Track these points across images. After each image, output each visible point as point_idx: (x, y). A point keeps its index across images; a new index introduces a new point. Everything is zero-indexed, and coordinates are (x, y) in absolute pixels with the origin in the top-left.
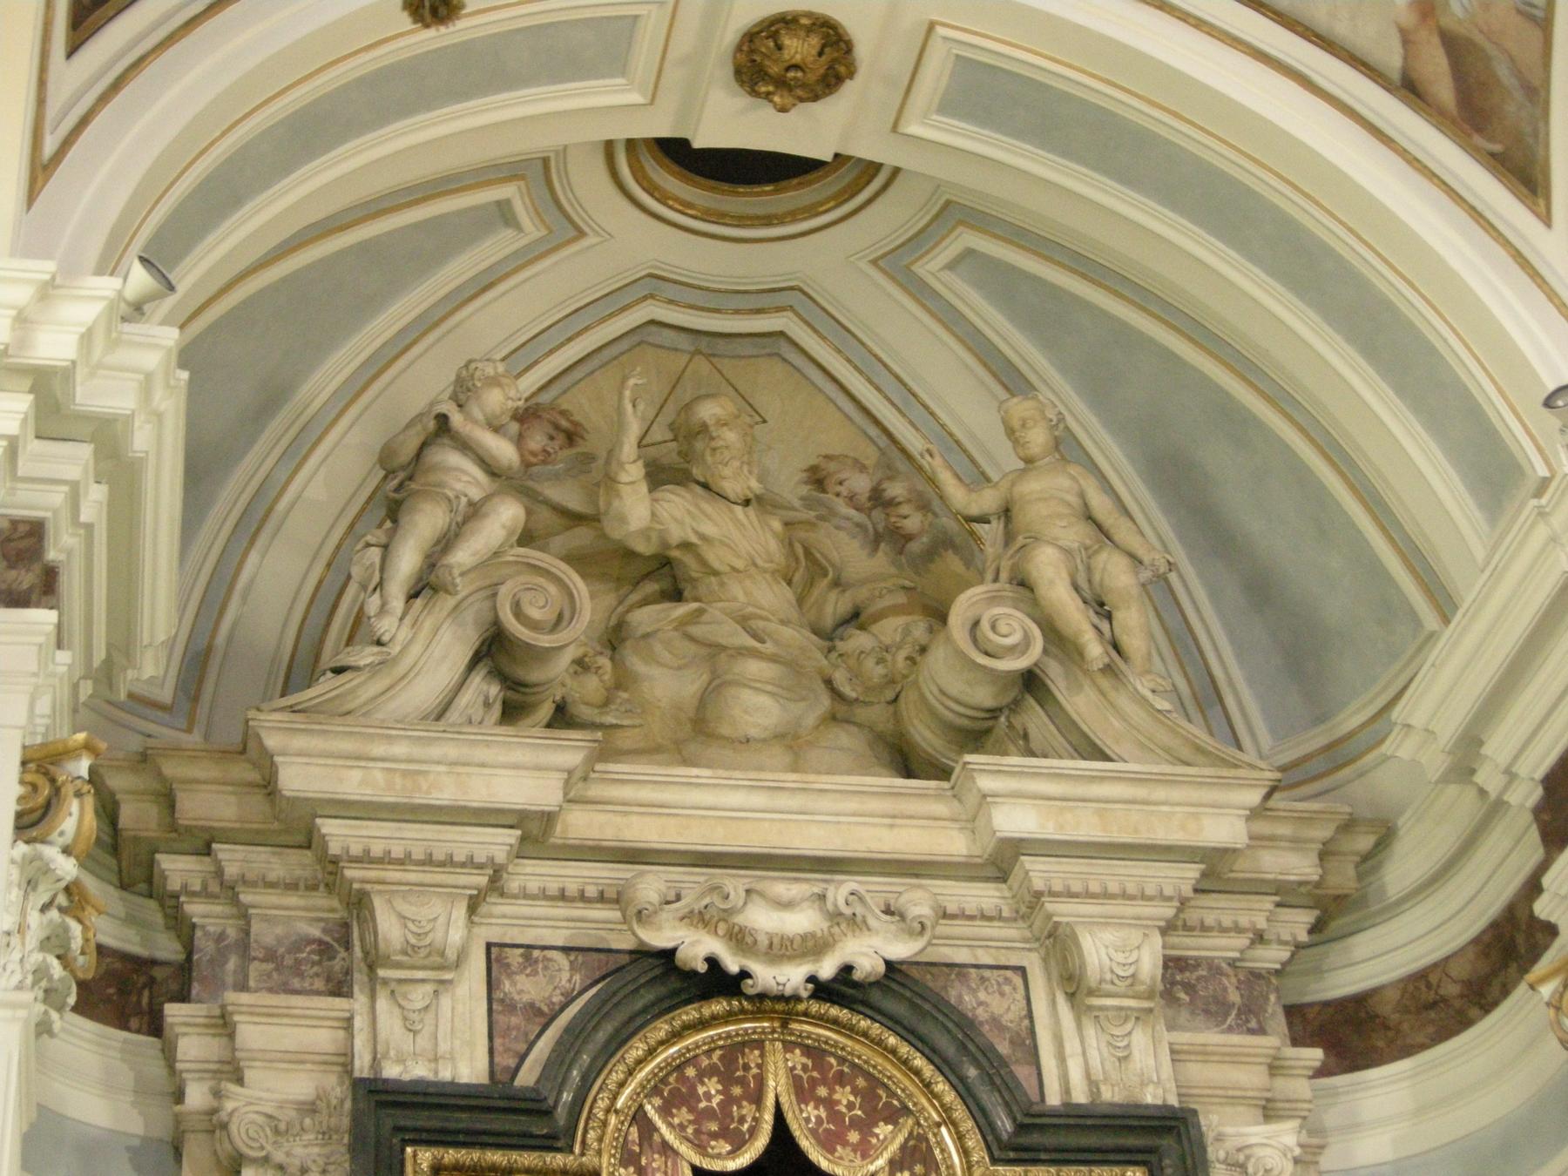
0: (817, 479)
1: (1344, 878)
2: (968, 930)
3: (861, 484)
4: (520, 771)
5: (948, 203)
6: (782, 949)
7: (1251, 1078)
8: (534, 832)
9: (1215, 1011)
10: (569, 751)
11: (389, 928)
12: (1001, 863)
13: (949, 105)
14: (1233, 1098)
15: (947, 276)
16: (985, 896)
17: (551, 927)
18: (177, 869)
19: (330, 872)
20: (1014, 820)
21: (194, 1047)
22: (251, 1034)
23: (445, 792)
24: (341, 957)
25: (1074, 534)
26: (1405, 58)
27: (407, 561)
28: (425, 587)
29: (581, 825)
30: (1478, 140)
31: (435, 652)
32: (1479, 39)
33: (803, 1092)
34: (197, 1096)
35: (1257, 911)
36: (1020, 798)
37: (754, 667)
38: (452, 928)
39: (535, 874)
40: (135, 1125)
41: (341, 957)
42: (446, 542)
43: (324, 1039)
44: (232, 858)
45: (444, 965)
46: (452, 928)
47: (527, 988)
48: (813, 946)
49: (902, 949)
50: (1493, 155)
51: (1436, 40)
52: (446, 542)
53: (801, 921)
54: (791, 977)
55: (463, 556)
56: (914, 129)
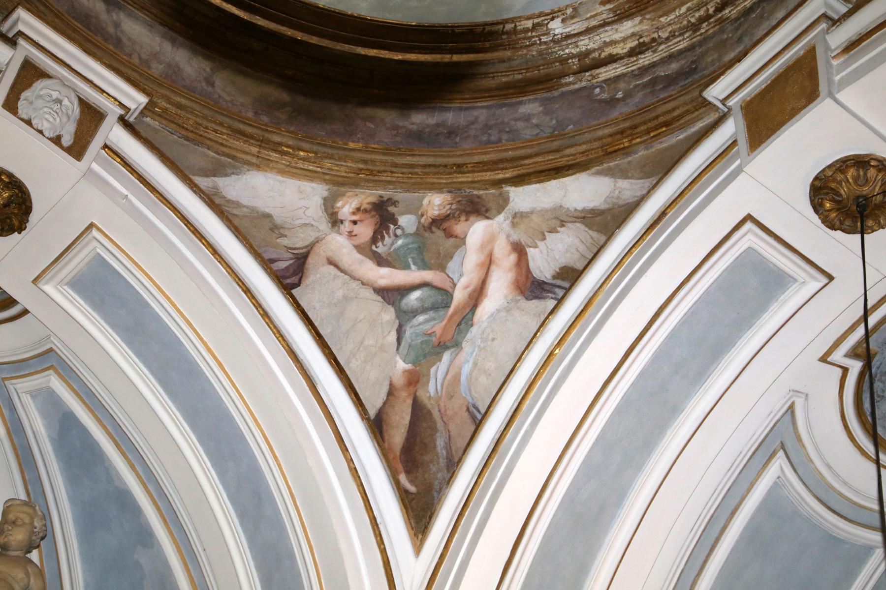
5: (51, 350)
13: (79, 284)
15: (27, 399)
26: (385, 404)
30: (403, 478)
32: (436, 414)
50: (407, 492)
51: (409, 402)
56: (49, 288)
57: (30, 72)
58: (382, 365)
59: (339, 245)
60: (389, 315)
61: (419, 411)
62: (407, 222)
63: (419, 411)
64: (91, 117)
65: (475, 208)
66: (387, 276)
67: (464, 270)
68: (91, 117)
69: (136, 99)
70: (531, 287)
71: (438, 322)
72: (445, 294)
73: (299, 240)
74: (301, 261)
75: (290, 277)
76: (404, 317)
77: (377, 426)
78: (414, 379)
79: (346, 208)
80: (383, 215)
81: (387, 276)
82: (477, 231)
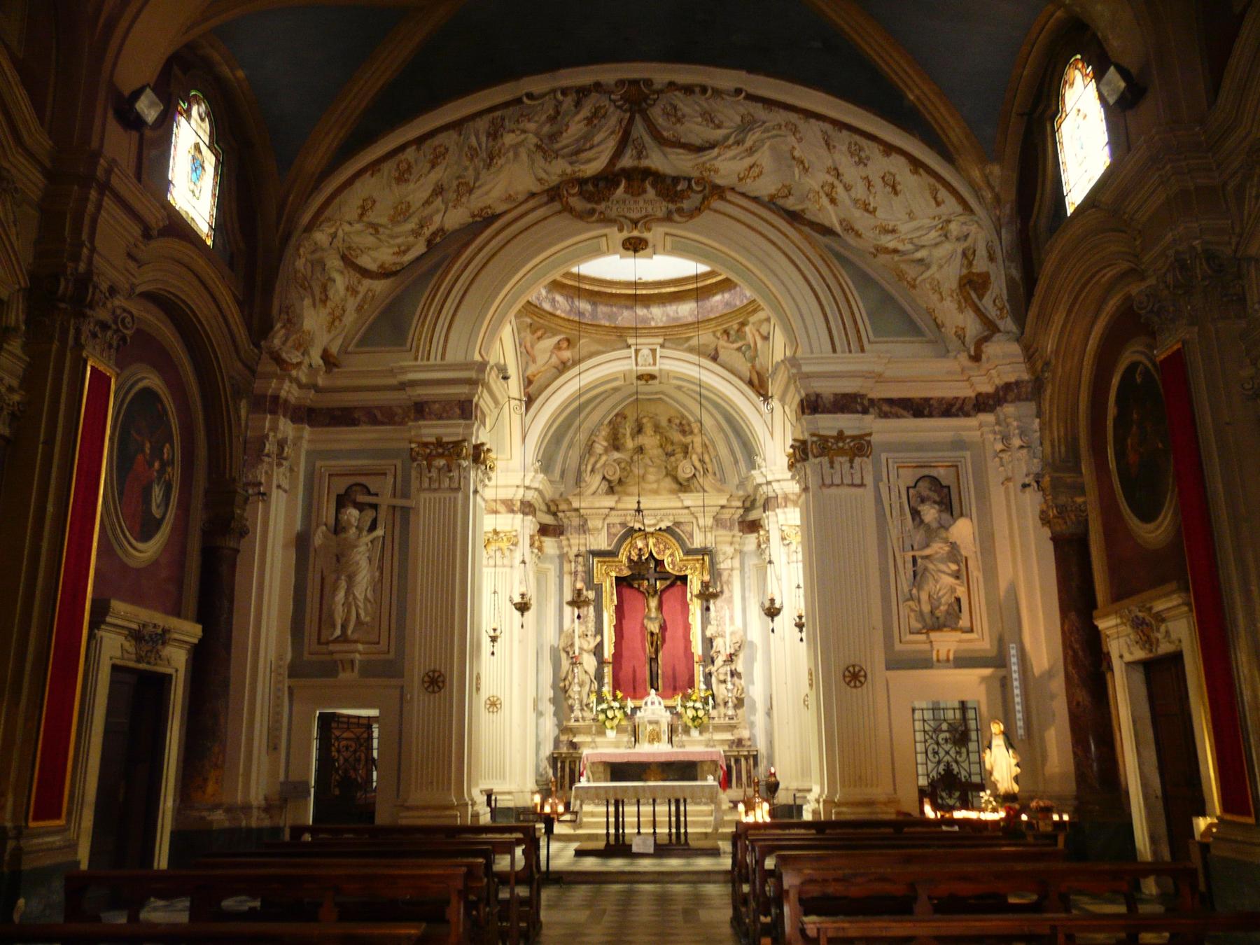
0: (670, 421)
1: (748, 504)
2: (684, 517)
3: (677, 421)
4: (609, 501)
6: (649, 526)
7: (729, 539)
8: (611, 509)
9: (724, 527)
10: (615, 498)
11: (590, 524)
12: (688, 508)
14: (725, 543)
16: (686, 511)
17: (617, 520)
18: (560, 514)
19: (581, 516)
20: (687, 503)
21: (565, 543)
22: (572, 541)
23: (597, 505)
24: (583, 529)
25: (699, 450)
27: (589, 468)
28: (593, 471)
29: (620, 506)
31: (594, 482)
33: (655, 545)
34: (565, 550)
35: (733, 511)
36: (689, 499)
37: (651, 470)
38: (599, 523)
39: (613, 513)
40: (558, 552)
41: (583, 529)
42: (596, 462)
43: (582, 541)
44: (568, 514)
45: (599, 530)
46: (599, 523)
47: (613, 530)
48: (654, 525)
49: (670, 524)
52: (596, 462)
53: (652, 522)
54: (652, 530)
55: (598, 466)
57: (637, 351)
58: (745, 368)
59: (722, 343)
60: (741, 355)
61: (758, 373)
62: (732, 332)
63: (758, 373)
64: (653, 351)
65: (743, 324)
66: (736, 345)
67: (749, 336)
68: (653, 351)
69: (660, 340)
70: (766, 338)
71: (751, 353)
72: (749, 346)
73: (713, 346)
74: (716, 350)
75: (714, 359)
76: (744, 354)
77: (750, 383)
78: (753, 366)
79: (719, 334)
80: (726, 332)
81: (736, 345)
82: (747, 329)
